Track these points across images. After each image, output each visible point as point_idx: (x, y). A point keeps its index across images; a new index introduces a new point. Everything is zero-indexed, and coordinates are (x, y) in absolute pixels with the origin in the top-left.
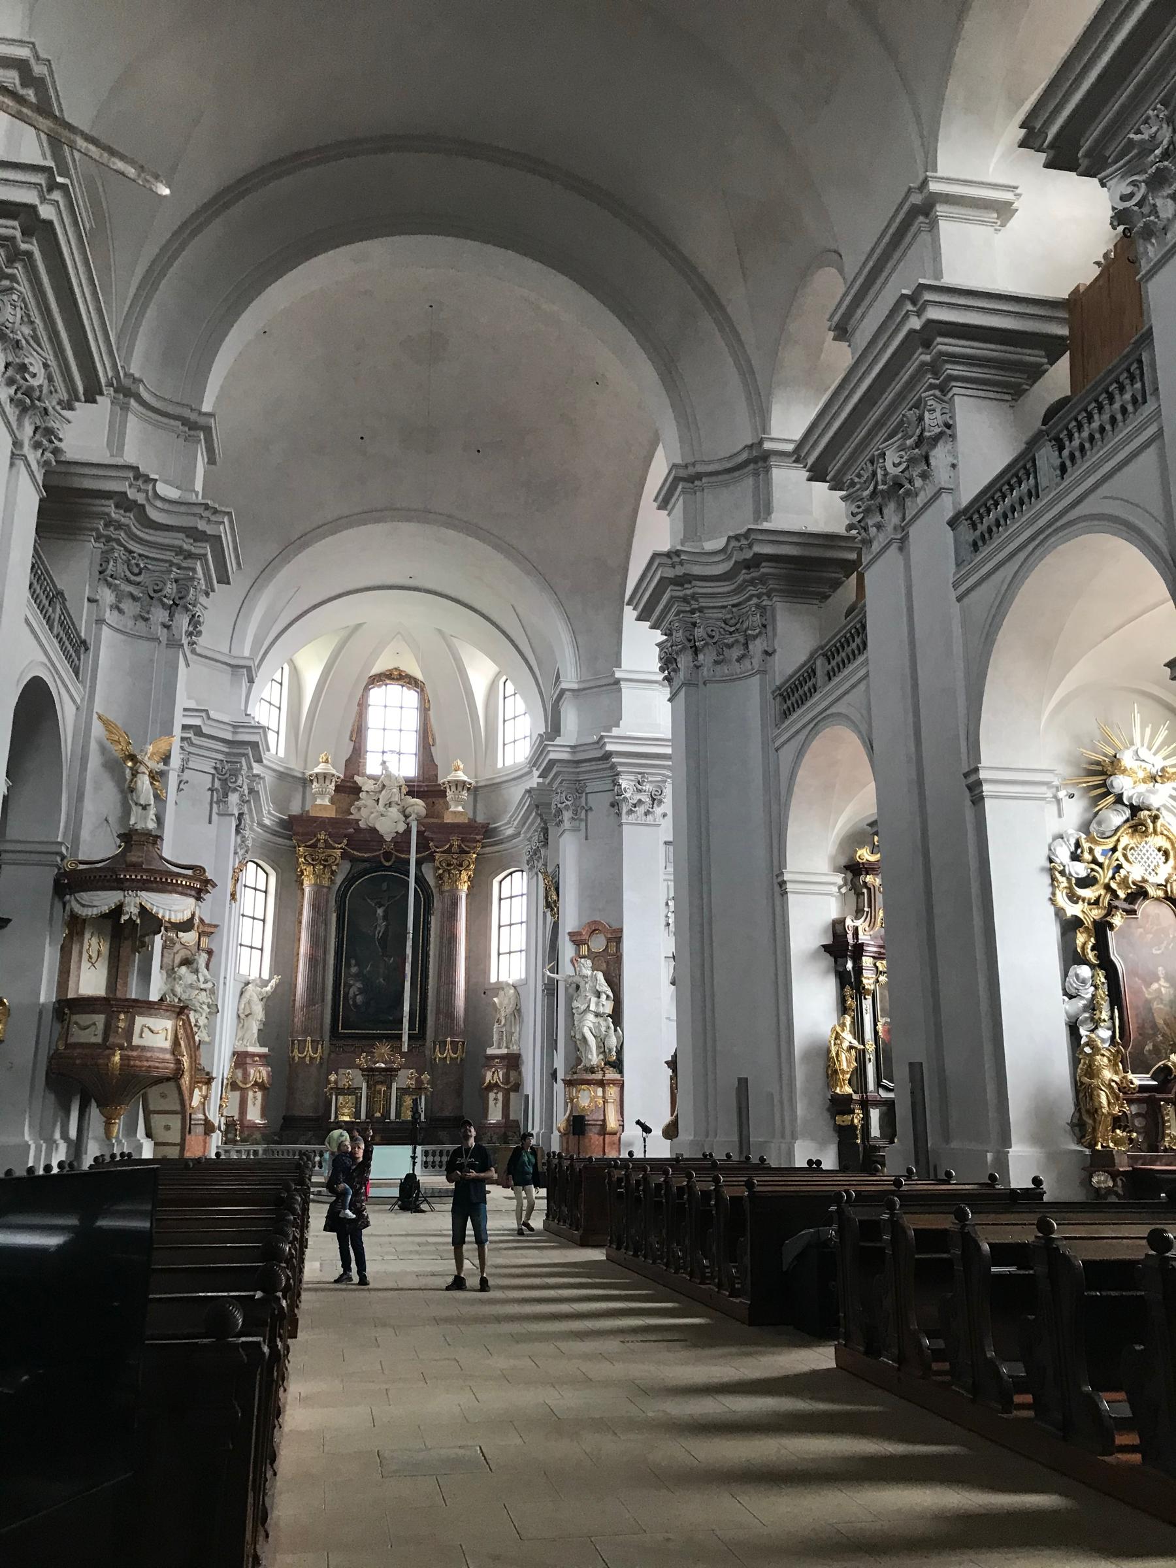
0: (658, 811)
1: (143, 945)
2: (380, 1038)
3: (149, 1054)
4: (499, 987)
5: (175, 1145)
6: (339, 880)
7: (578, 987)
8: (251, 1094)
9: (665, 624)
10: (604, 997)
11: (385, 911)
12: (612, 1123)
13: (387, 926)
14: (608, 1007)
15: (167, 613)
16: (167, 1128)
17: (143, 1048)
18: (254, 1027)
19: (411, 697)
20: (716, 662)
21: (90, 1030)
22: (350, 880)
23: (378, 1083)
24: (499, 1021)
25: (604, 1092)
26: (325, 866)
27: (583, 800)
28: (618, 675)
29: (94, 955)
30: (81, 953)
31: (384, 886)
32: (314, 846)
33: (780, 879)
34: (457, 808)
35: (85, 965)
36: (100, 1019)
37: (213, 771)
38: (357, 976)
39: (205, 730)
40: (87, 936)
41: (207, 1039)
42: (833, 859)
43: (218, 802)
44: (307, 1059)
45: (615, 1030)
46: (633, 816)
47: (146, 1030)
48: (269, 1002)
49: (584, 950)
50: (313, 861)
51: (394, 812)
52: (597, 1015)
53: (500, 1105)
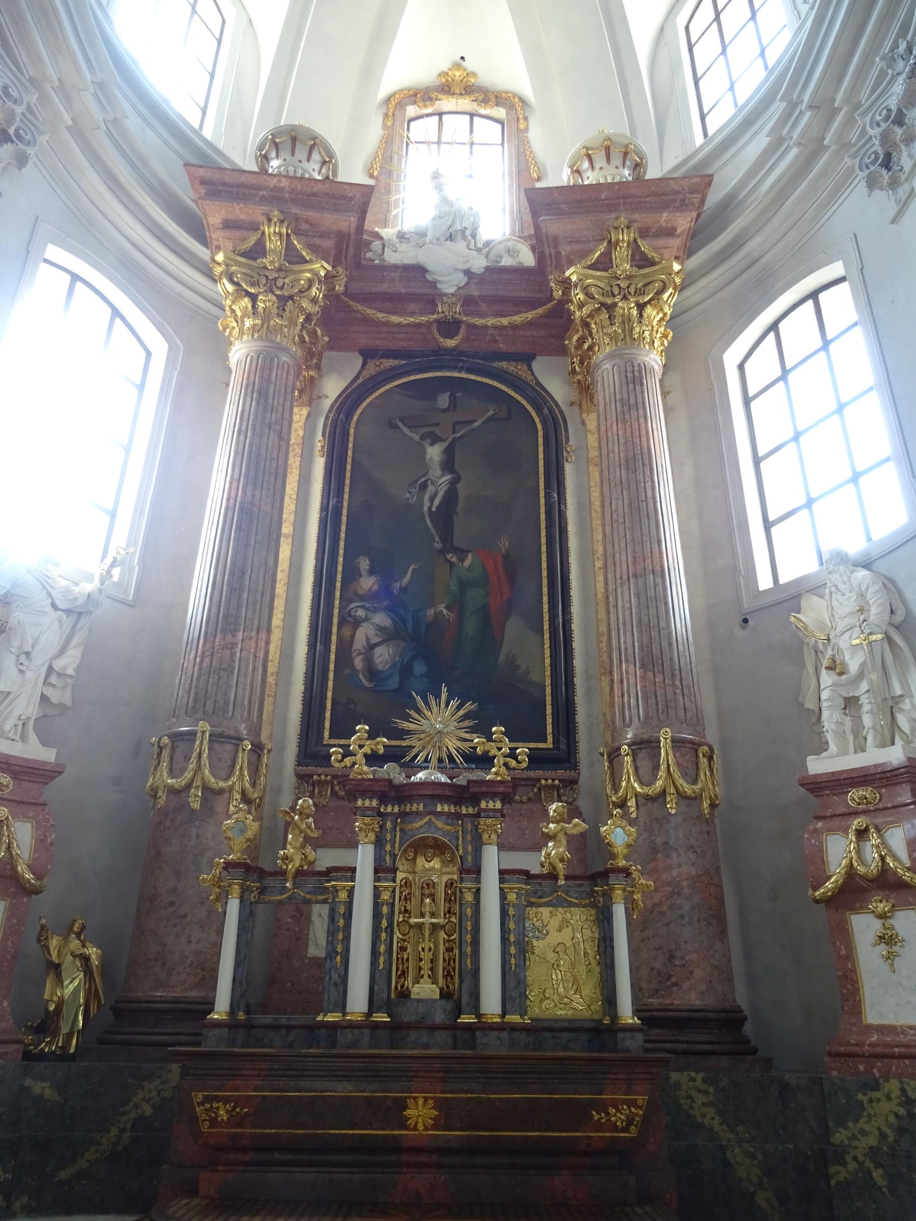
4: (791, 597)
6: (333, 388)
13: (453, 483)
23: (423, 847)
26: (283, 300)
31: (443, 400)
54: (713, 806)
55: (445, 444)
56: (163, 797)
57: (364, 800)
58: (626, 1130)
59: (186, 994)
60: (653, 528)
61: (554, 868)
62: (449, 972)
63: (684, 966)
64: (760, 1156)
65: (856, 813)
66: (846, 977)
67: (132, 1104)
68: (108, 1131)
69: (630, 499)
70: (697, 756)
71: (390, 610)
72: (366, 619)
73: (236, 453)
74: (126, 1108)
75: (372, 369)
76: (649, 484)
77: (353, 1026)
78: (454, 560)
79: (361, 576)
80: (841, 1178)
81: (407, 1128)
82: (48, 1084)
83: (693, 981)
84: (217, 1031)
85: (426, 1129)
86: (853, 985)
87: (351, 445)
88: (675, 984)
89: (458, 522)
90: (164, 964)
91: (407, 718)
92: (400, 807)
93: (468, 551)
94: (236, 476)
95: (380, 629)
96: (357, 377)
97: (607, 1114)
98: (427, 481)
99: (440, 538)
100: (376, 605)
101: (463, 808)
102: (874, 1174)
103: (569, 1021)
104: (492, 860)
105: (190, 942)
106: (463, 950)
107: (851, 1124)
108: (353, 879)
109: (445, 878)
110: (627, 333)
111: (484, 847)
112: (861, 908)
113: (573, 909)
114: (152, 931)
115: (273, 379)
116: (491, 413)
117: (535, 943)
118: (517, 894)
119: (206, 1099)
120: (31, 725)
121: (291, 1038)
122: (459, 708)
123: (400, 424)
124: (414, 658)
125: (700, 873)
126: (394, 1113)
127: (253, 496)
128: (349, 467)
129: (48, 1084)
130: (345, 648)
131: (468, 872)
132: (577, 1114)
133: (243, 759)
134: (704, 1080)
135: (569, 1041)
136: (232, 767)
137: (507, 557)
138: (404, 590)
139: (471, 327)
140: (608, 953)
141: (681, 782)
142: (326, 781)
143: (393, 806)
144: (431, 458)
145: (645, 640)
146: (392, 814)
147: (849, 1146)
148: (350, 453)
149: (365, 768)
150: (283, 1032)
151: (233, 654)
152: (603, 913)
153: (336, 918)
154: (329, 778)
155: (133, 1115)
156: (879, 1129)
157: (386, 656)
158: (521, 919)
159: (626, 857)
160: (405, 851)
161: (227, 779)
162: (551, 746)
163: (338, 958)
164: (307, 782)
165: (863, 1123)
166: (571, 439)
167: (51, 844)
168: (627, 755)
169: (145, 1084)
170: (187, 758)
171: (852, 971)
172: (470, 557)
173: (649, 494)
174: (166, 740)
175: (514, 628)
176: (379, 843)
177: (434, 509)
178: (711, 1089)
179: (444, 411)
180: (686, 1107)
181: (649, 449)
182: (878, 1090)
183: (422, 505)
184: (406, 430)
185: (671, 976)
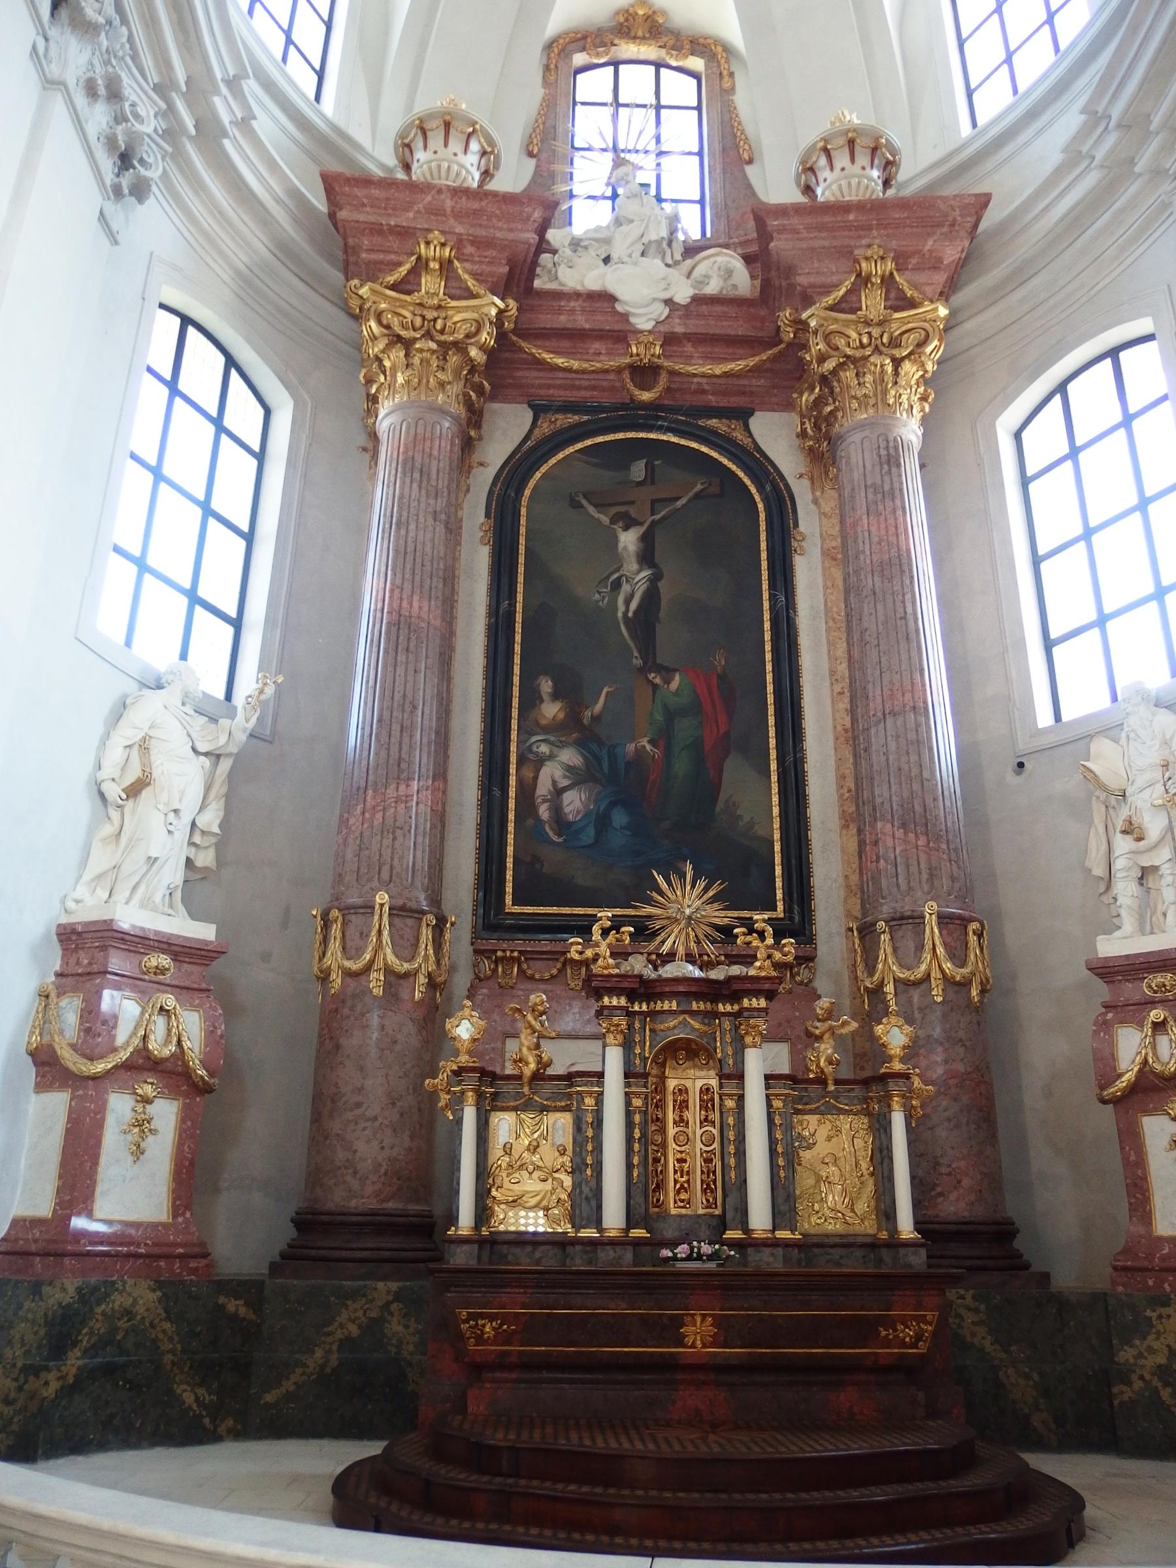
8: (120, 1106)
11: (647, 542)
13: (654, 581)
31: (638, 470)
44: (376, 983)
48: (244, 775)
54: (983, 992)
55: (641, 530)
56: (337, 980)
57: (610, 998)
58: (915, 1346)
59: (384, 1205)
60: (914, 653)
61: (822, 1072)
62: (708, 1185)
63: (950, 1174)
64: (1036, 1376)
65: (1152, 1003)
66: (1136, 1185)
67: (336, 1324)
68: (313, 1352)
69: (886, 615)
70: (966, 934)
71: (580, 744)
72: (551, 757)
73: (396, 551)
74: (330, 1329)
76: (908, 597)
77: (613, 1243)
78: (658, 681)
79: (542, 701)
80: (1126, 1397)
81: (685, 1346)
82: (242, 1302)
83: (961, 1190)
84: (466, 1247)
85: (704, 1346)
86: (1143, 1194)
87: (523, 530)
88: (941, 1194)
89: (662, 632)
90: (355, 1173)
91: (650, 902)
92: (648, 1005)
93: (676, 670)
94: (398, 582)
95: (570, 769)
96: (527, 438)
97: (895, 1330)
98: (619, 578)
99: (640, 652)
100: (563, 739)
101: (720, 1005)
102: (1162, 1393)
103: (841, 1236)
104: (758, 1063)
105: (382, 1148)
106: (726, 1161)
107: (1137, 1342)
108: (601, 1084)
109: (699, 1084)
110: (879, 398)
111: (747, 1050)
112: (1155, 1109)
113: (842, 1117)
114: (338, 1135)
115: (435, 453)
116: (699, 487)
117: (801, 1153)
118: (784, 1101)
119: (471, 1317)
120: (178, 895)
121: (537, 1255)
122: (706, 890)
123: (584, 502)
124: (613, 804)
125: (969, 1070)
126: (672, 1330)
127: (420, 608)
128: (521, 559)
129: (242, 1302)
130: (527, 792)
131: (729, 1077)
132: (864, 1331)
133: (426, 934)
134: (973, 1297)
135: (841, 1257)
136: (416, 945)
137: (721, 677)
138: (596, 719)
139: (672, 373)
140: (885, 1164)
141: (948, 966)
142: (512, 958)
143: (640, 1004)
144: (625, 548)
145: (906, 794)
146: (641, 1013)
147: (1135, 1365)
148: (522, 540)
149: (611, 961)
150: (529, 1248)
151: (408, 809)
152: (878, 1121)
153: (584, 1127)
154: (516, 954)
155: (339, 1335)
156: (1168, 1346)
157: (578, 804)
158: (789, 1127)
159: (902, 1060)
160: (656, 1056)
161: (411, 959)
162: (782, 915)
163: (589, 1172)
164: (488, 958)
165: (1151, 1340)
166: (801, 522)
167: (222, 1036)
168: (884, 932)
169: (349, 1303)
170: (364, 936)
171: (1141, 1179)
172: (677, 678)
173: (909, 610)
174: (335, 913)
175: (734, 771)
176: (627, 1046)
177: (630, 614)
178: (983, 1307)
179: (639, 484)
180: (954, 1327)
181: (908, 551)
182: (1169, 1306)
183: (616, 610)
184: (591, 510)
185: (935, 1185)
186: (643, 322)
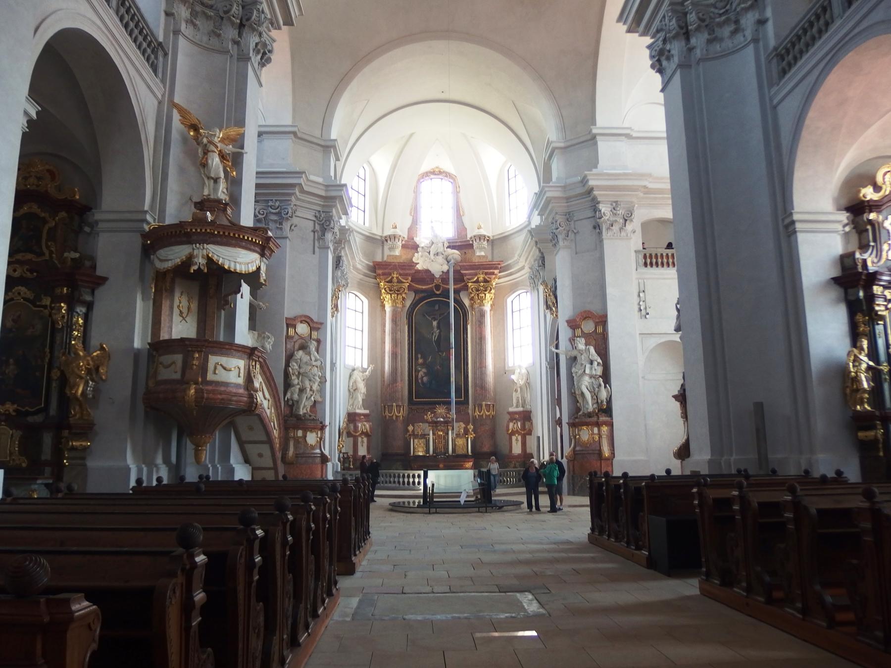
0: (629, 227)
1: (227, 303)
2: (439, 403)
3: (223, 389)
5: (269, 469)
6: (408, 303)
7: (575, 358)
8: (360, 439)
9: (656, 24)
10: (595, 363)
11: (438, 324)
12: (606, 452)
13: (440, 333)
14: (599, 371)
15: (236, 32)
16: (260, 455)
17: (217, 383)
18: (360, 398)
19: (446, 186)
20: (709, 42)
21: (171, 367)
22: (414, 305)
24: (516, 391)
25: (599, 430)
27: (572, 226)
28: (595, 131)
29: (185, 311)
30: (171, 308)
31: (437, 307)
32: (390, 281)
33: (787, 221)
34: (481, 253)
35: (176, 318)
36: (178, 358)
37: (314, 219)
38: (423, 365)
39: (306, 188)
40: (177, 295)
41: (320, 399)
42: (836, 201)
43: (319, 239)
44: (394, 418)
45: (605, 387)
46: (610, 233)
47: (219, 367)
48: (368, 382)
49: (578, 332)
50: (390, 291)
51: (440, 259)
52: (591, 377)
53: (520, 443)
75: (417, 298)
130: (417, 377)
186: (437, 276)
